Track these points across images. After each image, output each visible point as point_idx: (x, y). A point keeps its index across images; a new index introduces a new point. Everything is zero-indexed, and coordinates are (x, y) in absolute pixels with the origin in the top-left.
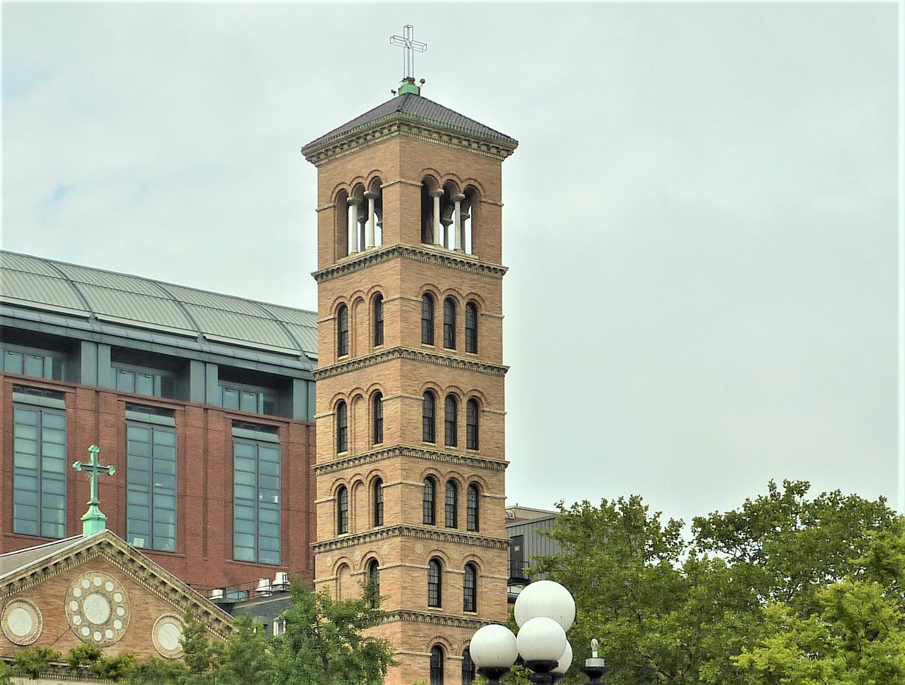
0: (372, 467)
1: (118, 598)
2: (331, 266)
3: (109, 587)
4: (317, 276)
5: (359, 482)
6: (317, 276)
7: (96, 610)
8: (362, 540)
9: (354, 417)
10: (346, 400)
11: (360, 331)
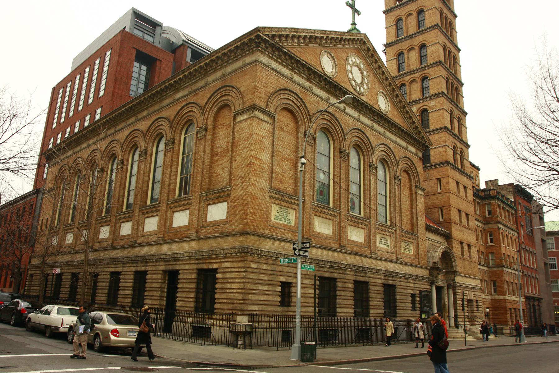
0: (422, 73)
1: (365, 73)
2: (393, 6)
3: (362, 66)
4: (384, 12)
5: (414, 81)
6: (384, 12)
7: (356, 75)
8: (417, 102)
9: (408, 58)
10: (404, 51)
11: (409, 26)
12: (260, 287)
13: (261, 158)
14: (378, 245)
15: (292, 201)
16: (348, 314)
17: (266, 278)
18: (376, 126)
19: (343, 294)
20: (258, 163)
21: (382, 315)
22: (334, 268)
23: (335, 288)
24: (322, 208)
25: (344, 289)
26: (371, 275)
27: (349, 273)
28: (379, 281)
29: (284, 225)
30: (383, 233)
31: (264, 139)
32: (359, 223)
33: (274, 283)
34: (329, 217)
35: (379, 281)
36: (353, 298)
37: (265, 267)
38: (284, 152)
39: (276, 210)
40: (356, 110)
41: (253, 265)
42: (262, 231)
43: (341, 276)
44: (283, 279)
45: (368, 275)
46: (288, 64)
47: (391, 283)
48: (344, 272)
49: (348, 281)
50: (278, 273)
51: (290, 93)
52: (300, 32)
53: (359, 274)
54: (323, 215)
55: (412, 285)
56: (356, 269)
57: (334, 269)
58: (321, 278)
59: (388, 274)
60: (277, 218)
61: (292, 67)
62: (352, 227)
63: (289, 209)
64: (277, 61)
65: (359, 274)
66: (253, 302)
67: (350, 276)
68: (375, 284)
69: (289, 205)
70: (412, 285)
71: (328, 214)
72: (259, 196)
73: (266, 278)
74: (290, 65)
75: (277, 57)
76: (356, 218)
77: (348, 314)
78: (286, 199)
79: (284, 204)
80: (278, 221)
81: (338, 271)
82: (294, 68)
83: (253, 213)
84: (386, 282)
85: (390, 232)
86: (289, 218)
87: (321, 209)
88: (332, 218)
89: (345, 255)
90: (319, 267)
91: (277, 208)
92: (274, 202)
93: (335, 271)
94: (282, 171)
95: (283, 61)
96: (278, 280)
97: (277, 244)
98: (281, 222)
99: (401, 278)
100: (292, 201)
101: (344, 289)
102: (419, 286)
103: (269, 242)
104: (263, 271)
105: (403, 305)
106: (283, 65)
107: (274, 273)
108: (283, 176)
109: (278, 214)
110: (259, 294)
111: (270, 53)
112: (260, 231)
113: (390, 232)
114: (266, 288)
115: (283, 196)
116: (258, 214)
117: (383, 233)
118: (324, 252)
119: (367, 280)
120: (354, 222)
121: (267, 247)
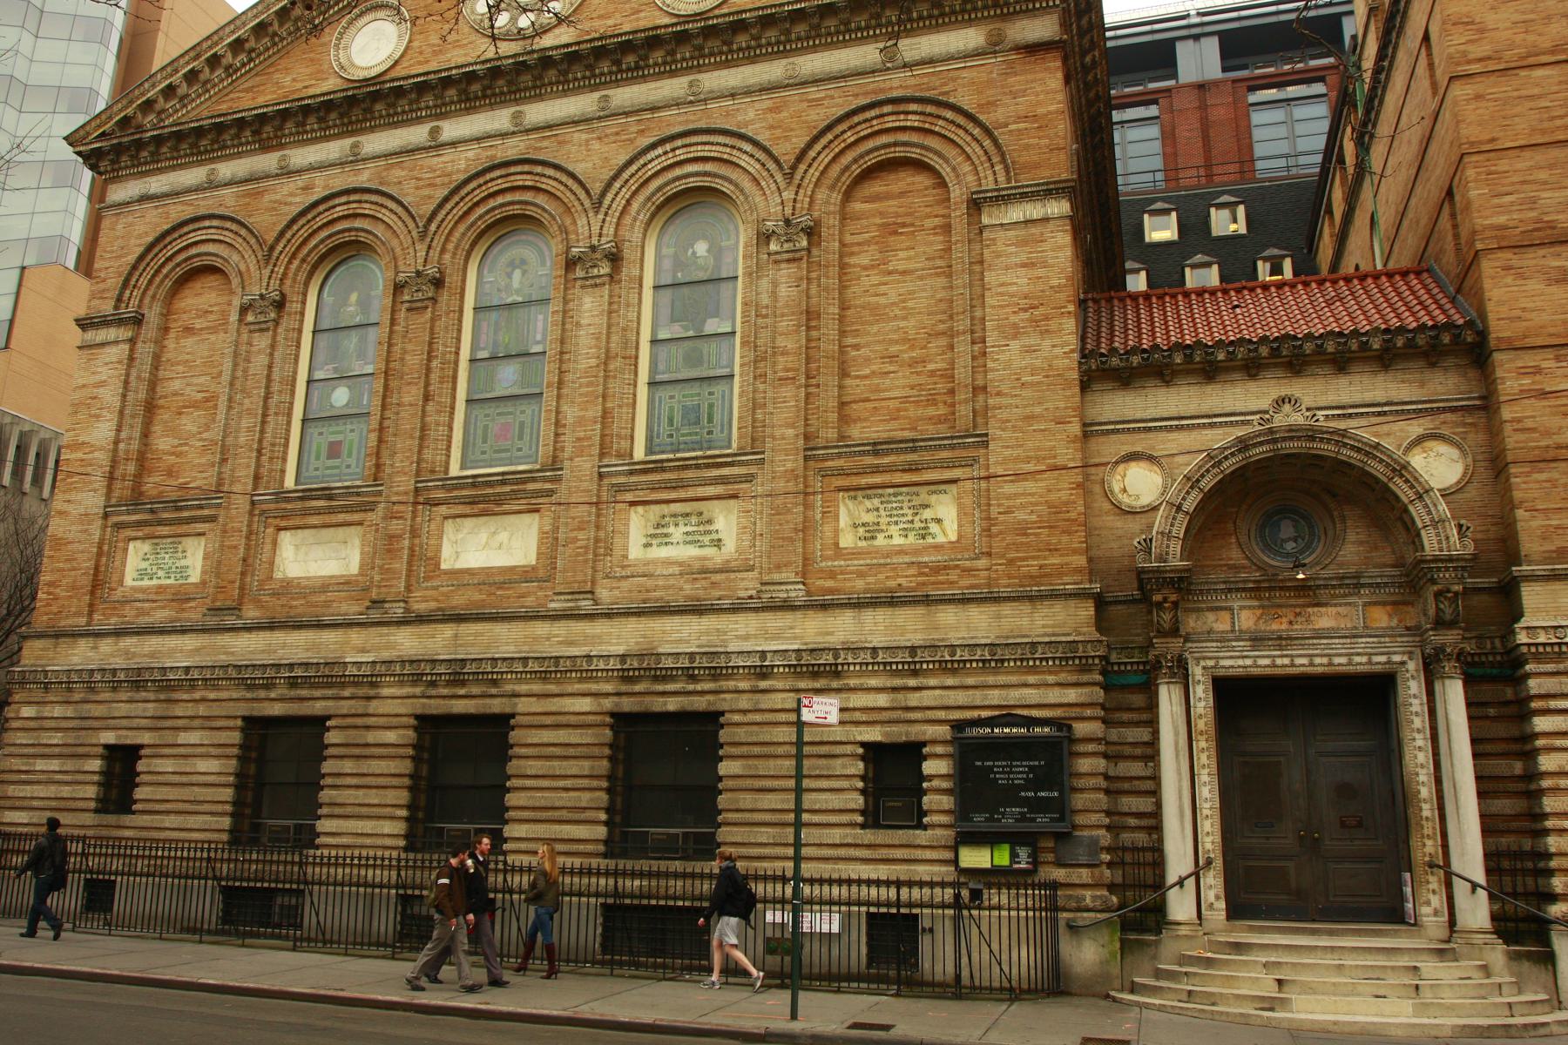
12: (40, 765)
13: (87, 439)
14: (635, 552)
15: (186, 514)
16: (368, 841)
17: (57, 738)
18: (626, 95)
19: (348, 766)
20: (80, 455)
21: (601, 848)
22: (308, 682)
23: (318, 752)
24: (301, 498)
25: (357, 751)
26: (524, 688)
27: (386, 692)
28: (585, 704)
29: (160, 587)
30: (673, 495)
31: (101, 390)
32: (499, 500)
33: (81, 750)
34: (341, 517)
35: (585, 704)
36: (407, 781)
37: (58, 711)
38: (188, 390)
39: (141, 554)
40: (492, 106)
41: (27, 711)
42: (69, 622)
43: (345, 707)
44: (109, 738)
45: (509, 688)
46: (186, 155)
47: (700, 704)
48: (361, 692)
49: (382, 721)
50: (96, 724)
51: (197, 225)
52: (210, 48)
53: (445, 691)
54: (314, 520)
55: (882, 700)
56: (417, 672)
57: (314, 686)
58: (255, 726)
59: (642, 668)
60: (142, 574)
61: (200, 153)
62: (469, 522)
63: (184, 540)
64: (161, 171)
65: (445, 691)
66: (17, 804)
67: (397, 703)
68: (548, 720)
69: (184, 528)
70: (882, 700)
71: (331, 511)
72: (71, 536)
73: (57, 738)
74: (192, 154)
75: (153, 162)
76: (474, 485)
77: (368, 841)
78: (166, 515)
79: (165, 530)
80: (146, 583)
81: (329, 692)
82: (206, 151)
83: (51, 584)
84: (628, 705)
85: (723, 480)
86: (183, 563)
87: (299, 505)
88: (356, 517)
89: (385, 630)
90: (250, 688)
91: (146, 547)
92: (134, 534)
93: (318, 693)
94: (176, 442)
95: (173, 158)
96: (94, 741)
97: (106, 646)
98: (155, 582)
99: (763, 673)
100: (186, 514)
101: (357, 751)
102: (960, 697)
103: (83, 645)
104: (53, 724)
105: (747, 800)
106: (173, 168)
107: (87, 724)
108: (178, 455)
109: (145, 565)
110: (39, 782)
111: (133, 166)
112: (63, 623)
113: (723, 480)
114: (54, 765)
115: (152, 511)
116: (64, 582)
117: (673, 495)
118: (279, 637)
119: (496, 706)
120: (473, 502)
121: (75, 659)
